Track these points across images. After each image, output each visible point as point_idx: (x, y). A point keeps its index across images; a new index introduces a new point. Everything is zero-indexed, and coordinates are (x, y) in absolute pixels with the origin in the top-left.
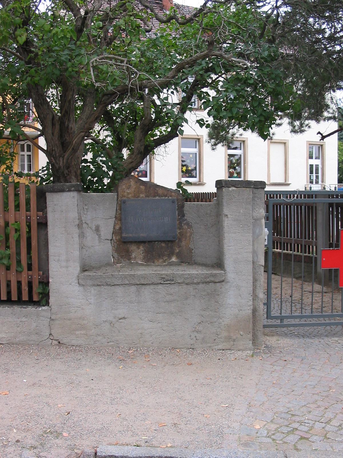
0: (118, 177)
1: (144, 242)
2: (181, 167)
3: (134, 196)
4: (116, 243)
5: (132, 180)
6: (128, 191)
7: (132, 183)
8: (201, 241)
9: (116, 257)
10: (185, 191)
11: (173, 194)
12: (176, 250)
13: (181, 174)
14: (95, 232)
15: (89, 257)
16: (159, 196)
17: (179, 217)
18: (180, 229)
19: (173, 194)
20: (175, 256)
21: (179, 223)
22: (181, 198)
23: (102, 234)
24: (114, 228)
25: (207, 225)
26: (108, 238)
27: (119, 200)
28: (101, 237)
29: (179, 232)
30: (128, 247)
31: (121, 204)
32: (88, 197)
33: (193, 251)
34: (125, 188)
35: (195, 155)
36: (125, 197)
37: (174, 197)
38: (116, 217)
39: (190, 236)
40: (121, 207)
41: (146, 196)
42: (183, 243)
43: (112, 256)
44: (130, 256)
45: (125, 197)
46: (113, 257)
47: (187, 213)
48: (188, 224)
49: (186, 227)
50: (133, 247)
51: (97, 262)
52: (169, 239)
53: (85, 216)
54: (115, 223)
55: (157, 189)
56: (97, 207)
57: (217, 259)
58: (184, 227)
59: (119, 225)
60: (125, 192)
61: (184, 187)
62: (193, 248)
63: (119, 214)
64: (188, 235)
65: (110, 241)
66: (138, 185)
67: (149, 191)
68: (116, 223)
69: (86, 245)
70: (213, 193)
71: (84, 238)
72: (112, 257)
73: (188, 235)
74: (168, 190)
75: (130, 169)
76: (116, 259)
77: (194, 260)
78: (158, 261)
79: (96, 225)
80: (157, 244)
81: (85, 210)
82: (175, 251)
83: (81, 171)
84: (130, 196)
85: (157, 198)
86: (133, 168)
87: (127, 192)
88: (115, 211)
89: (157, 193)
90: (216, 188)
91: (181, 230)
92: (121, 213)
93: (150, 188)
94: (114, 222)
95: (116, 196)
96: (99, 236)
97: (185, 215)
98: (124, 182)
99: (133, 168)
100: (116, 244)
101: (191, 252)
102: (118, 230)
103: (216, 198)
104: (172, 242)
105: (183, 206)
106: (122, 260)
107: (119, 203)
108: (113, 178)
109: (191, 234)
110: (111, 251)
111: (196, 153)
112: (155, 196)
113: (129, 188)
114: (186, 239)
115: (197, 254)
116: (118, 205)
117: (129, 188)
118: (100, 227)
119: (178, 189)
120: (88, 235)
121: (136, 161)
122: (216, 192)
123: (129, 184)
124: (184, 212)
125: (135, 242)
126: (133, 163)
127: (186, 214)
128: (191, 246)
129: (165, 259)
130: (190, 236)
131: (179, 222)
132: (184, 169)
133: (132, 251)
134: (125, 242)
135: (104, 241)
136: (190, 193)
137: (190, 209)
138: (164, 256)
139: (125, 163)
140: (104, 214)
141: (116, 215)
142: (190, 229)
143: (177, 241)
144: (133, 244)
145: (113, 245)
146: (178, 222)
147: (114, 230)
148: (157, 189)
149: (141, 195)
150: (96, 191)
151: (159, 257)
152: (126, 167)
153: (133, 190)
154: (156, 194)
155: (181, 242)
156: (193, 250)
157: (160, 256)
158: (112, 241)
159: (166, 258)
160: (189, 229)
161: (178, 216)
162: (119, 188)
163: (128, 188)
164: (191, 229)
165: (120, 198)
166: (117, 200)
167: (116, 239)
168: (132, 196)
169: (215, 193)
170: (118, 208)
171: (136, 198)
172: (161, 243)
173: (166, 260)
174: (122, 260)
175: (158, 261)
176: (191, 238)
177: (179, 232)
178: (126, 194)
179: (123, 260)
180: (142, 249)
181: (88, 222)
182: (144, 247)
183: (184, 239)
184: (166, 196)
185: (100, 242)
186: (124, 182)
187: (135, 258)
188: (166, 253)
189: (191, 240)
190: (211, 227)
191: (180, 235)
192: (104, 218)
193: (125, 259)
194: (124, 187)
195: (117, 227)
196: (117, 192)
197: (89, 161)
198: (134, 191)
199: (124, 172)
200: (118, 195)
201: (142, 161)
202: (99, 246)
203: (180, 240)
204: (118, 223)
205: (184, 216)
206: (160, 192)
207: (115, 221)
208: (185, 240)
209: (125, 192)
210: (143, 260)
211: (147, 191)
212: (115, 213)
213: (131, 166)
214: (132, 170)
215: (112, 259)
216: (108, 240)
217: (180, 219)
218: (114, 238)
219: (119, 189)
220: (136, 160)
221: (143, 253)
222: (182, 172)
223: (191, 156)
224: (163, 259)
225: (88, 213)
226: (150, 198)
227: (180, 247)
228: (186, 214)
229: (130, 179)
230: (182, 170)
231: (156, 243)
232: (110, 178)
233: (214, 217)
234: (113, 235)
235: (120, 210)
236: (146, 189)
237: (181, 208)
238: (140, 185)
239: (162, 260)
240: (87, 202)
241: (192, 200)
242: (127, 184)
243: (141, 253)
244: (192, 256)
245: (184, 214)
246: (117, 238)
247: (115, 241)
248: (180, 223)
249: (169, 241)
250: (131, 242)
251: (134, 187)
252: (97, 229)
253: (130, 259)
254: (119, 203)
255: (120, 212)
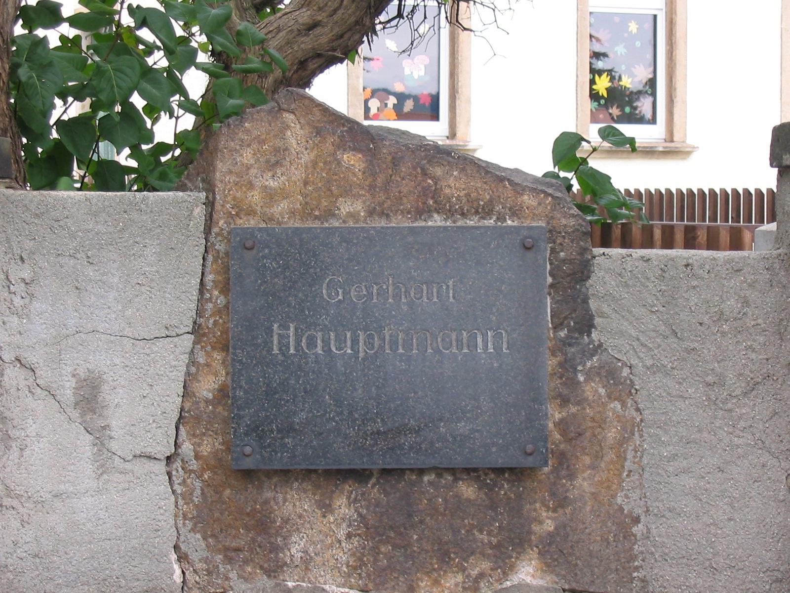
0: (232, 102)
1: (359, 475)
2: (588, 76)
3: (306, 212)
4: (199, 477)
5: (292, 116)
6: (272, 184)
7: (295, 133)
8: (685, 471)
9: (194, 557)
10: (597, 183)
11: (527, 199)
12: (541, 523)
13: (588, 105)
14: (75, 414)
15: (36, 556)
16: (450, 213)
17: (563, 334)
18: (565, 401)
19: (527, 199)
20: (534, 553)
21: (561, 365)
22: (572, 222)
23: (117, 422)
24: (187, 393)
25: (721, 382)
26: (149, 450)
27: (215, 230)
28: (114, 446)
29: (562, 420)
30: (266, 502)
31: (227, 254)
32: (37, 216)
33: (638, 530)
34: (252, 161)
35: (649, 26)
36: (251, 212)
37: (535, 217)
38: (197, 330)
39: (622, 442)
40: (226, 269)
41: (371, 213)
42: (583, 484)
43: (176, 548)
44: (275, 549)
45: (251, 212)
46: (182, 558)
47: (605, 309)
48: (609, 374)
49: (602, 391)
50: (294, 503)
51: (88, 584)
52: (500, 463)
53: (15, 319)
54: (192, 362)
55: (438, 171)
56: (90, 271)
57: (778, 581)
58: (589, 394)
59: (216, 375)
60: (251, 186)
61: (596, 164)
62: (639, 511)
63: (218, 312)
64: (611, 434)
65: (160, 468)
66: (328, 147)
67: (388, 182)
68: (201, 360)
69: (19, 490)
70: (759, 192)
71: (8, 448)
72: (174, 557)
73: (611, 434)
74: (501, 179)
75: (303, 64)
76: (199, 566)
77: (643, 580)
78: (436, 582)
79: (83, 376)
80: (431, 483)
81: (19, 288)
82: (535, 528)
83: (15, 67)
84: (280, 208)
85: (437, 221)
86: (319, 55)
87: (265, 188)
88: (195, 293)
89: (436, 194)
90: (775, 171)
91: (573, 409)
92: (226, 307)
93: (396, 162)
94: (185, 358)
95: (199, 212)
96: (100, 436)
97: (597, 321)
98: (248, 132)
99: (319, 55)
100: (198, 484)
101: (628, 536)
102: (207, 401)
103: (773, 226)
104: (517, 473)
105: (582, 271)
106: (233, 575)
107: (221, 247)
108: (209, 112)
109: (630, 429)
110: (167, 521)
111: (655, 17)
112: (422, 212)
113: (277, 163)
114: (598, 456)
115: (663, 544)
116: (210, 258)
117: (275, 161)
118: (105, 388)
119: (562, 174)
120: (32, 429)
121: (335, 17)
122: (775, 191)
123: (279, 143)
124: (593, 304)
125: (309, 473)
126: (318, 31)
127: (602, 315)
128: (628, 500)
129: (474, 572)
130: (622, 442)
131: (560, 358)
132: (603, 84)
133: (286, 521)
134: (248, 475)
135: (128, 466)
136: (627, 191)
137: (626, 285)
138: (473, 553)
139: (279, 30)
140: (129, 313)
141: (200, 312)
142: (624, 405)
143: (546, 469)
144: (296, 485)
145: (179, 489)
146: (551, 363)
147: (187, 406)
148: (438, 171)
149: (346, 207)
150: (107, 177)
151: (444, 557)
152: (280, 49)
153: (297, 174)
154: (431, 201)
155: (572, 476)
156: (637, 520)
157: (447, 553)
158: (178, 464)
159: (486, 565)
160: (617, 405)
161: (557, 327)
162: (219, 165)
163: (272, 166)
164: (630, 402)
165: (221, 223)
166: (207, 231)
167: (197, 457)
168: (292, 213)
169: (770, 191)
170: (210, 277)
171: (317, 224)
172: (456, 480)
173: (481, 575)
174: (233, 575)
175: (436, 582)
176: (630, 455)
177: (557, 416)
178: (255, 197)
179: (240, 576)
180: (344, 510)
181: (31, 358)
182: (356, 500)
183: (587, 460)
184: (486, 211)
185: (103, 469)
186: (248, 132)
187: (307, 562)
188: (484, 537)
189: (628, 464)
190: (745, 394)
191: (564, 433)
192: (128, 331)
193: (249, 569)
194: (247, 156)
195: (206, 387)
196: (210, 188)
197: (66, 12)
198: (306, 183)
199: (271, 79)
200: (210, 204)
201: (367, 21)
202: (99, 491)
203: (564, 463)
204: (208, 365)
205: (586, 325)
206: (454, 185)
207: (192, 352)
208: (593, 467)
209: (251, 186)
210: (349, 575)
211: (380, 180)
212: (193, 306)
213: (306, 43)
214: (311, 66)
215: (176, 567)
216: (149, 457)
217: (566, 343)
218: (187, 448)
219: (221, 167)
220: (335, 11)
221: (349, 536)
222: (594, 96)
223: (633, 27)
224: (464, 570)
225: (36, 305)
226: (399, 222)
227: (562, 503)
228: (602, 315)
229: (281, 109)
230: (591, 89)
231: (426, 478)
232: (188, 106)
233: (761, 339)
234: (183, 431)
235: (225, 289)
236: (370, 171)
237: (574, 278)
238: (341, 146)
239: (460, 578)
240: (29, 244)
241: (636, 231)
242: (263, 142)
243: (341, 534)
244: (633, 558)
245: (592, 317)
246: (206, 449)
247: (194, 465)
248: (568, 368)
249: (499, 471)
250: (286, 475)
251: (306, 158)
252: (89, 398)
253: (274, 570)
254: (221, 247)
255: (221, 301)
